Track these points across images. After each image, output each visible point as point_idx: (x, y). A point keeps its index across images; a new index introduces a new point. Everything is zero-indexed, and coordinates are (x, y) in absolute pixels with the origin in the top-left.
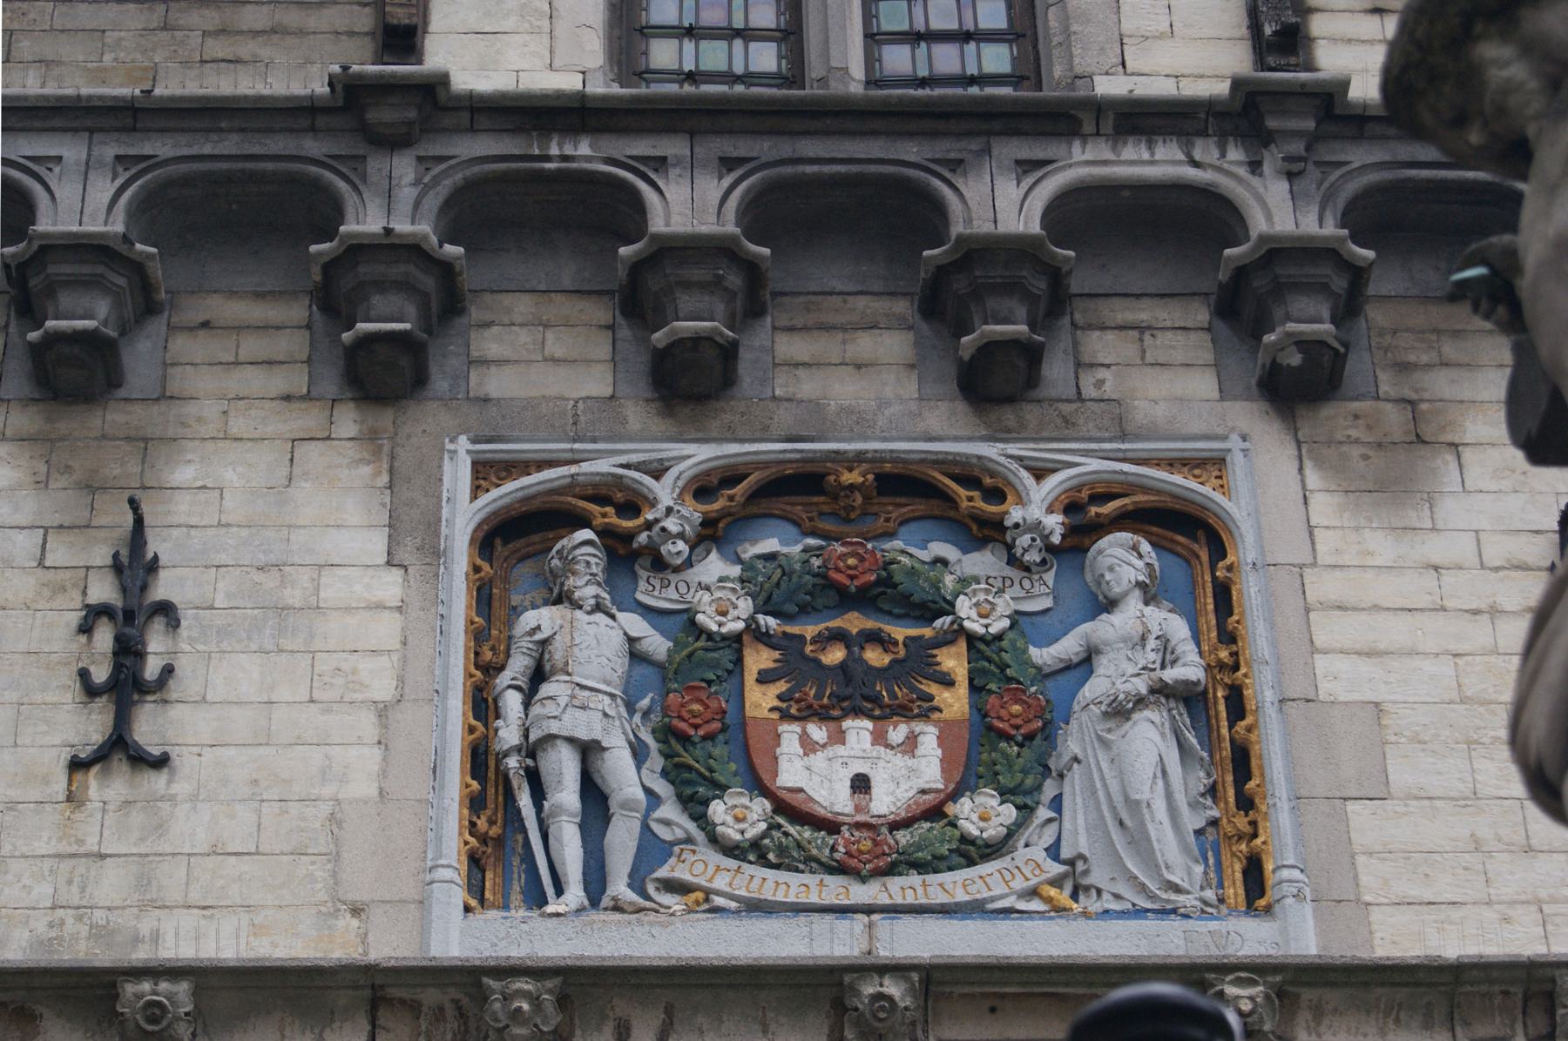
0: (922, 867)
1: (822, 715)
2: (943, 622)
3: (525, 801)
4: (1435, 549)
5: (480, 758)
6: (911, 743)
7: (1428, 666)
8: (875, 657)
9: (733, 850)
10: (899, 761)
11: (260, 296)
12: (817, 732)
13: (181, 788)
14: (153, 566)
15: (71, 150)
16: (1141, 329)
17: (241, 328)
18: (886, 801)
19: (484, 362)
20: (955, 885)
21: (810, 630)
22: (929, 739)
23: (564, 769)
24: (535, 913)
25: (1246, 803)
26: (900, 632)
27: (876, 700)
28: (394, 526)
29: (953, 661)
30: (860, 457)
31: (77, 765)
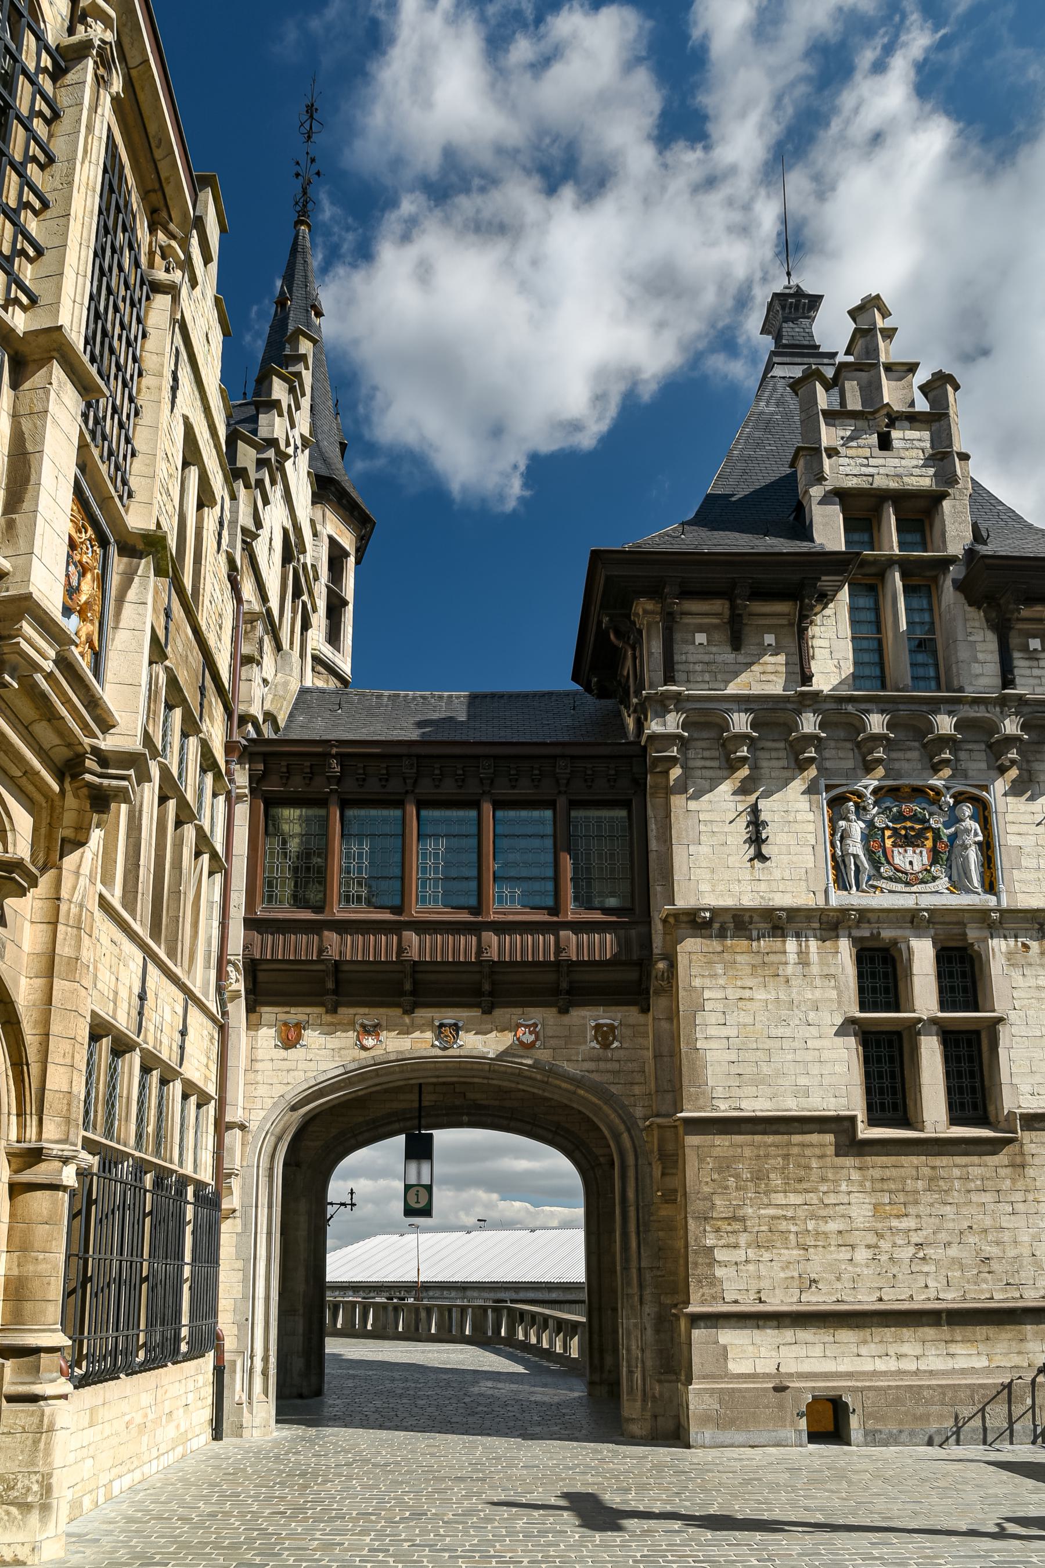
1: (901, 846)
2: (927, 825)
3: (842, 867)
5: (834, 856)
7: (1031, 837)
11: (774, 740)
12: (901, 850)
13: (773, 865)
16: (971, 750)
17: (770, 750)
18: (917, 867)
20: (931, 887)
21: (898, 826)
22: (924, 853)
24: (845, 893)
25: (989, 868)
26: (918, 827)
27: (912, 843)
29: (929, 835)
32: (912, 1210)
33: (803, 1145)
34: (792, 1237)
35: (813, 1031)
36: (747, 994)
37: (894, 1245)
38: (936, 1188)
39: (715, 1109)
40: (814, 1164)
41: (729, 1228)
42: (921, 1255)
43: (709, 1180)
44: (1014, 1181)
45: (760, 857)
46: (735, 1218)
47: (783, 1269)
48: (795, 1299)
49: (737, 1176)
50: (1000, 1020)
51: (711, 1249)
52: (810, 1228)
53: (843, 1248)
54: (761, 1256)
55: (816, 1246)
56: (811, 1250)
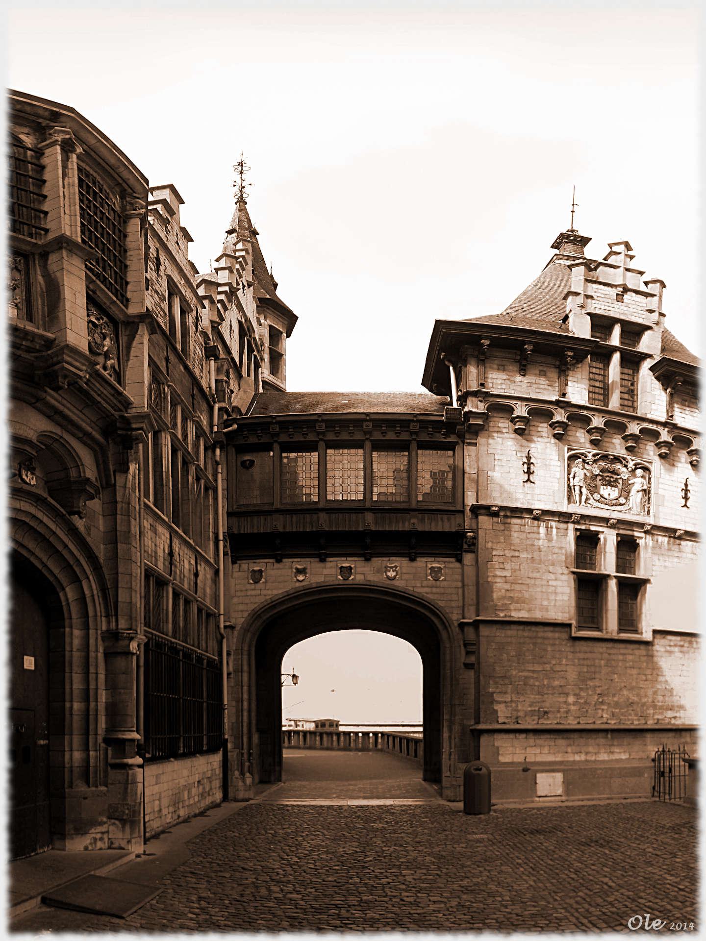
32: (597, 676)
33: (544, 638)
34: (536, 688)
35: (552, 576)
36: (517, 554)
37: (588, 695)
39: (497, 616)
40: (549, 649)
41: (502, 682)
42: (600, 700)
44: (647, 663)
45: (528, 480)
46: (505, 677)
47: (530, 706)
48: (535, 722)
49: (508, 654)
51: (493, 693)
52: (545, 683)
55: (547, 694)
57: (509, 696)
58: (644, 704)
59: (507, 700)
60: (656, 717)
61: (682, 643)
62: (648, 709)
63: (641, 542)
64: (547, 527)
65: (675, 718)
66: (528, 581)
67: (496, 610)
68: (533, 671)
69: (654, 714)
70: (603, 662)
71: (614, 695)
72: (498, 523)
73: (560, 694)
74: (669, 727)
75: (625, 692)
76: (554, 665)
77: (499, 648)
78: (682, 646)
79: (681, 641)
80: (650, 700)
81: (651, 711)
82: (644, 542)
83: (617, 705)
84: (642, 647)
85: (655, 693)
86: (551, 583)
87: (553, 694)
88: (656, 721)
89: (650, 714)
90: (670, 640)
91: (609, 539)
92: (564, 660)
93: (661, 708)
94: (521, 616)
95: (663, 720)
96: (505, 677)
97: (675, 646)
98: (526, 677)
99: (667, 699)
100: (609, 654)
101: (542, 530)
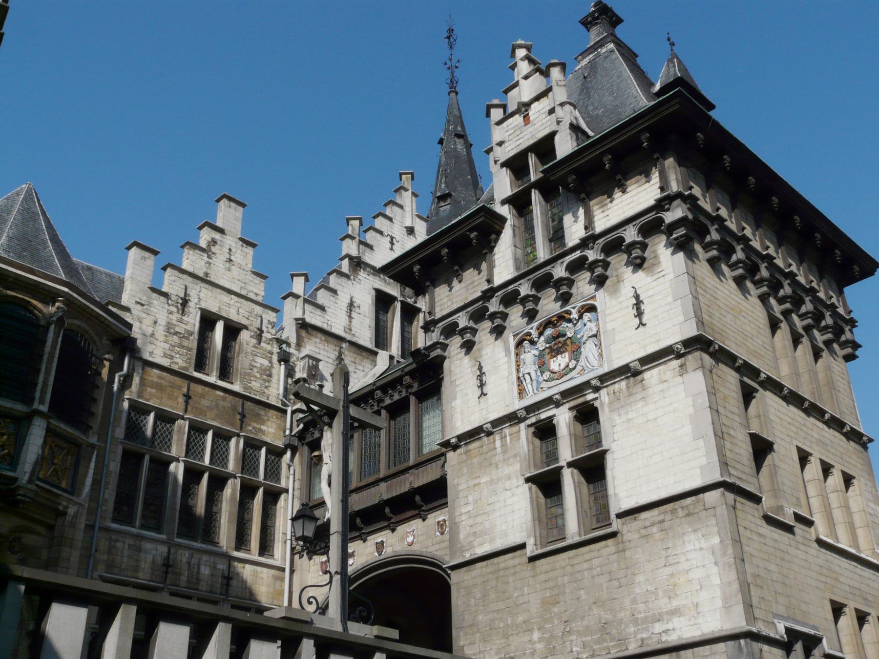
0: (566, 375)
1: (554, 357)
2: (566, 337)
4: (621, 299)
5: (519, 378)
6: (565, 357)
8: (560, 345)
9: (546, 381)
10: (564, 359)
12: (555, 359)
13: (489, 397)
14: (482, 368)
15: (460, 314)
18: (562, 367)
19: (512, 321)
23: (527, 377)
26: (561, 339)
28: (505, 350)
30: (554, 316)
31: (479, 398)
33: (506, 569)
35: (508, 493)
36: (477, 481)
38: (574, 580)
40: (511, 579)
42: (568, 629)
43: (462, 603)
44: (618, 562)
46: (472, 625)
50: (605, 452)
51: (463, 647)
53: (526, 633)
54: (486, 647)
56: (511, 638)
57: (478, 646)
58: (620, 622)
59: (475, 652)
60: (639, 636)
61: (661, 517)
62: (627, 626)
63: (597, 404)
64: (501, 438)
65: (666, 631)
66: (489, 508)
67: (463, 551)
68: (498, 611)
69: (636, 633)
70: (566, 578)
71: (582, 618)
72: (461, 454)
73: (525, 631)
74: (659, 646)
75: (595, 611)
76: (516, 598)
77: (467, 594)
78: (662, 521)
79: (660, 514)
80: (628, 613)
81: (632, 629)
82: (603, 399)
83: (587, 631)
84: (610, 542)
85: (634, 601)
86: (508, 502)
87: (517, 634)
88: (640, 643)
89: (630, 634)
90: (645, 519)
91: (563, 417)
92: (526, 589)
93: (645, 620)
94: (483, 551)
95: (650, 638)
96: (472, 625)
97: (653, 525)
98: (492, 620)
99: (650, 606)
100: (572, 565)
101: (498, 443)
